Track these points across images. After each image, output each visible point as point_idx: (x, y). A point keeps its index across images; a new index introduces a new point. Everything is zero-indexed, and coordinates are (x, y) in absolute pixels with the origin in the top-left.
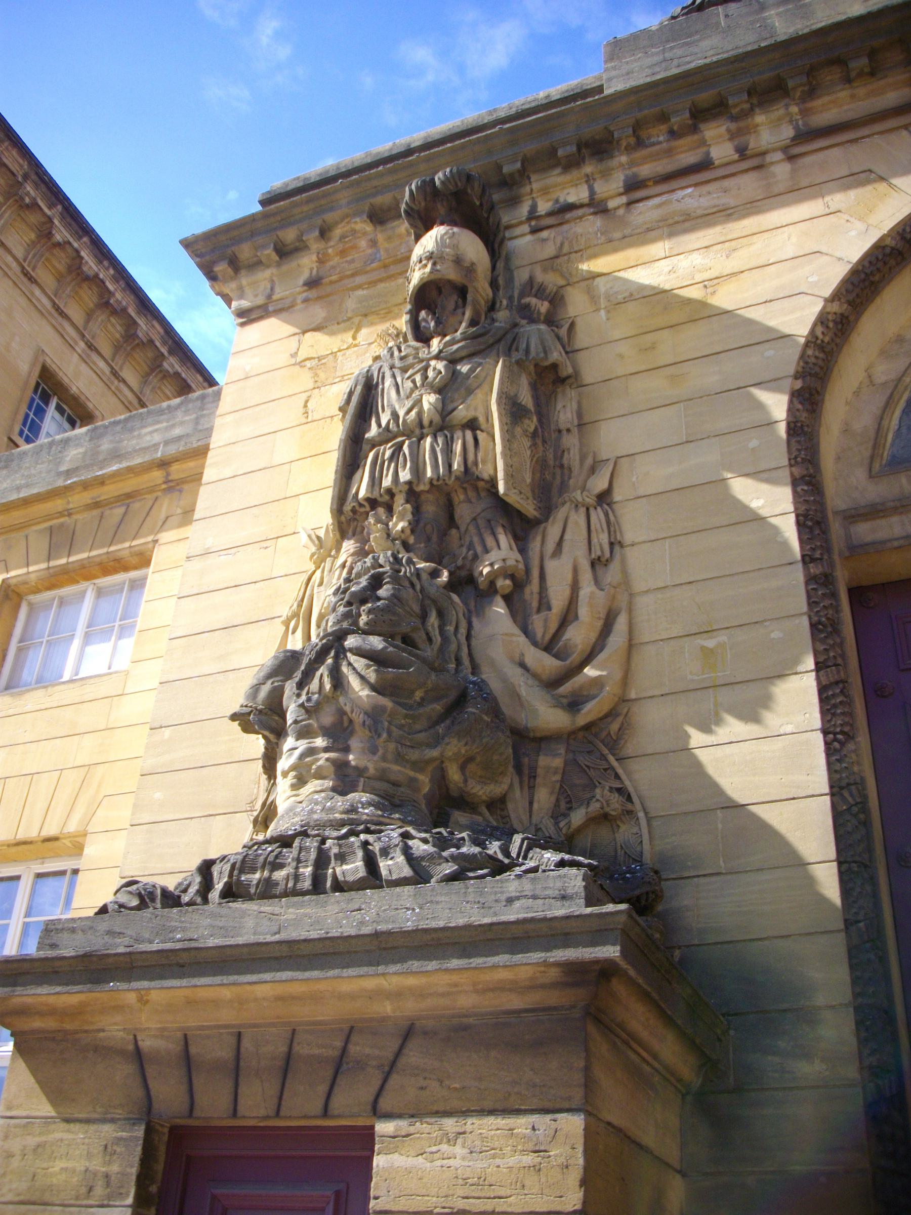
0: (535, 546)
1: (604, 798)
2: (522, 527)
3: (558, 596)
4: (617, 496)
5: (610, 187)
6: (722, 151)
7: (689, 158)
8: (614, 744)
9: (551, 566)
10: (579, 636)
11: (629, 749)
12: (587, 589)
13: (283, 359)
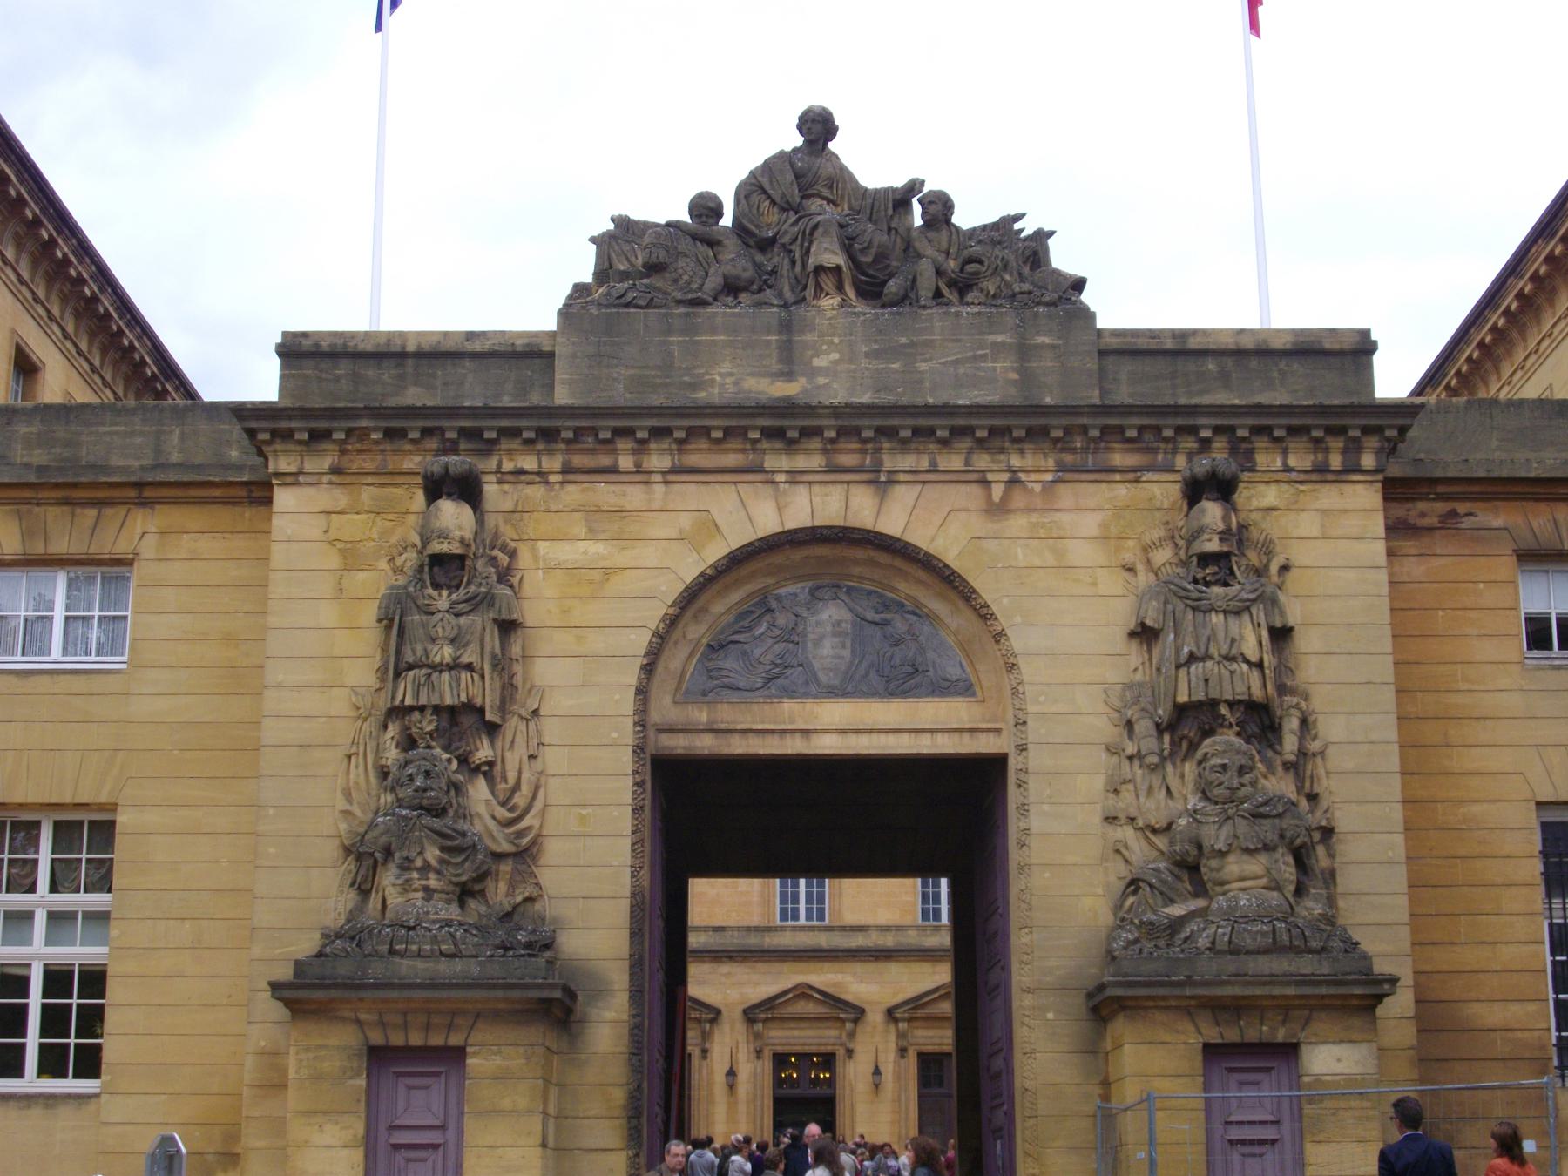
0: (499, 744)
1: (534, 891)
3: (512, 777)
5: (553, 463)
6: (626, 462)
7: (605, 460)
8: (535, 858)
9: (508, 754)
10: (520, 800)
11: (541, 862)
12: (526, 776)
13: (316, 533)
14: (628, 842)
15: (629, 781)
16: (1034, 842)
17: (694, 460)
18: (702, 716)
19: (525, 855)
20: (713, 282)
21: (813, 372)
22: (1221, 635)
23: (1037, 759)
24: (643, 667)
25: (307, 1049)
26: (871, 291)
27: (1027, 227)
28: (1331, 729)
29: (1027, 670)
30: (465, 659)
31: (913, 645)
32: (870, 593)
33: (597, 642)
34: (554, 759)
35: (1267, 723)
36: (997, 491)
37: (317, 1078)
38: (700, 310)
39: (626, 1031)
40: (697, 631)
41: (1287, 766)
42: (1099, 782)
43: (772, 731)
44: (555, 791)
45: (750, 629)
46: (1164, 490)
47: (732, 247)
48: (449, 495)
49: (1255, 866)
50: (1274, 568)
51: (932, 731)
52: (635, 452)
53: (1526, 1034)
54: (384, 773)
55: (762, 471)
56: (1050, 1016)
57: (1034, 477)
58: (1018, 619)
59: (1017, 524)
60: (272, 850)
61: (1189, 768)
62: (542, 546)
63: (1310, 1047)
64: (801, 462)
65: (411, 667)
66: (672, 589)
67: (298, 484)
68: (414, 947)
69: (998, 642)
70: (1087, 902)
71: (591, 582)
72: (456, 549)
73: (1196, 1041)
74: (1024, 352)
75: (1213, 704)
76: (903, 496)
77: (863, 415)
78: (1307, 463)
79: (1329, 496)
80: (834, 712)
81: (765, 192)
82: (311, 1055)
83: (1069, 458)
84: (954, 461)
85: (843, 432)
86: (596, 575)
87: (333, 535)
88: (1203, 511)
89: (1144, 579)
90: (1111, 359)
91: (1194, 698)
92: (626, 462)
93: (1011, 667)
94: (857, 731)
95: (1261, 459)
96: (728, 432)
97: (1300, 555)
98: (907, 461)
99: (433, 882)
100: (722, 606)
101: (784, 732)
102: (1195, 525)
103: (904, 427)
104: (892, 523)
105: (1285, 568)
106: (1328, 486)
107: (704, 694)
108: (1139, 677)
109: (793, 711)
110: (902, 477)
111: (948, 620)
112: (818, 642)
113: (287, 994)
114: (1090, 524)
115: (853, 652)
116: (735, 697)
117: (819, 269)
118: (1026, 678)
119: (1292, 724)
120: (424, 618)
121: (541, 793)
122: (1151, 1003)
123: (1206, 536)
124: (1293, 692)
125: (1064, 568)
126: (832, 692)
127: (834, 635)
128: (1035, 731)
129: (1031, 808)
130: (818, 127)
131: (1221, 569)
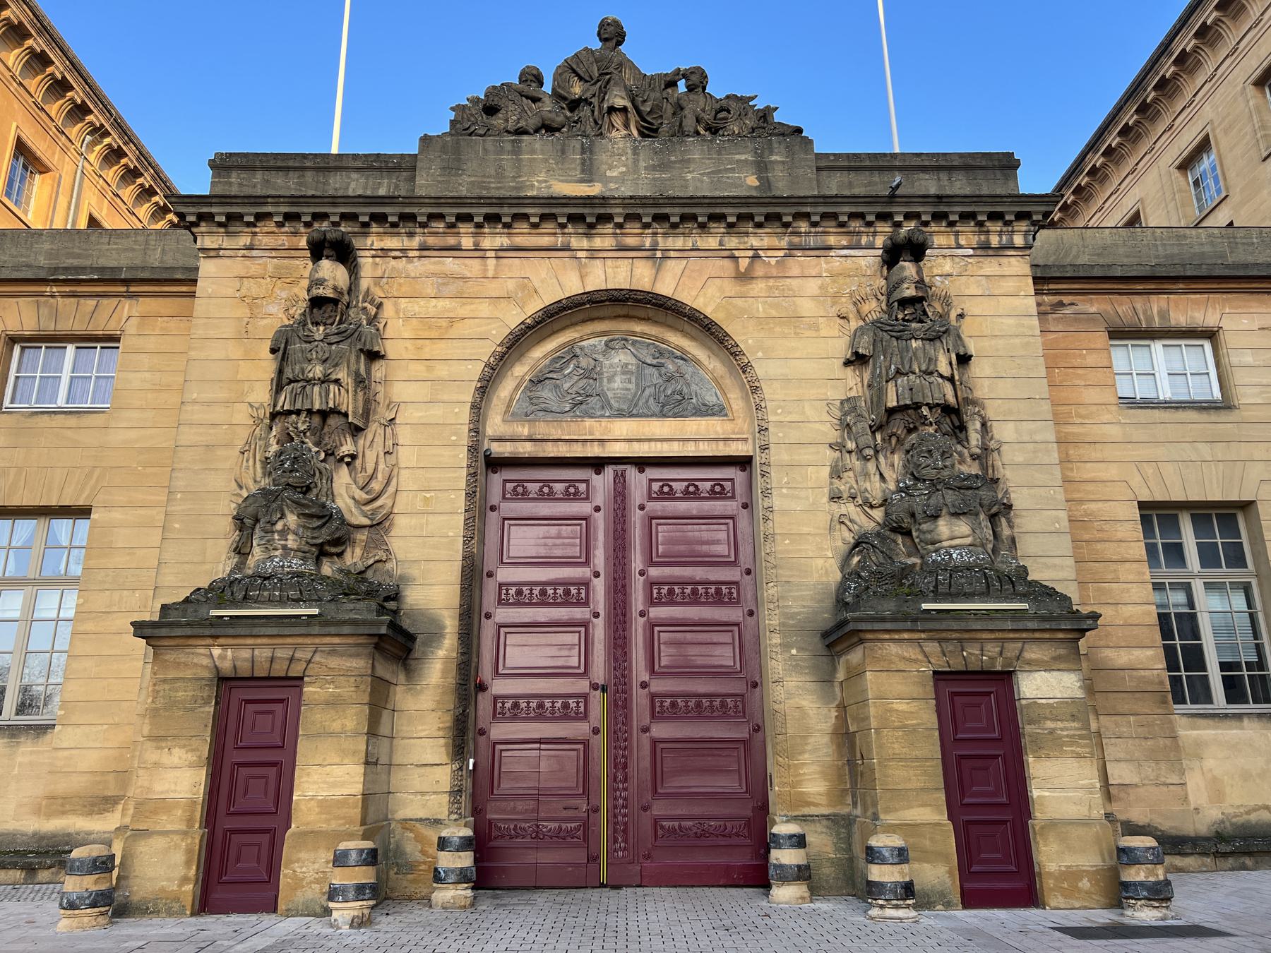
0: (361, 442)
1: (381, 555)
2: (356, 431)
3: (370, 467)
4: (397, 421)
6: (467, 242)
7: (451, 241)
8: (387, 531)
9: (368, 453)
10: (376, 486)
11: (392, 534)
12: (381, 466)
14: (461, 519)
15: (464, 472)
16: (777, 517)
17: (519, 241)
18: (525, 431)
19: (380, 525)
20: (532, 122)
21: (606, 180)
22: (920, 354)
23: (777, 455)
24: (477, 389)
25: (164, 681)
26: (649, 131)
27: (760, 104)
28: (1003, 432)
29: (767, 391)
30: (333, 377)
31: (681, 381)
32: (649, 345)
33: (442, 371)
34: (406, 456)
35: (957, 424)
36: (744, 263)
37: (171, 705)
38: (525, 137)
39: (454, 666)
40: (521, 370)
41: (974, 457)
42: (826, 471)
43: (577, 441)
44: (406, 479)
45: (561, 369)
46: (868, 260)
47: (547, 100)
48: (327, 257)
49: (963, 527)
50: (953, 315)
51: (695, 440)
52: (475, 235)
53: (1147, 673)
54: (266, 461)
55: (566, 248)
56: (794, 652)
57: (770, 253)
58: (760, 354)
59: (758, 287)
60: (177, 526)
61: (897, 459)
62: (403, 303)
63: (1025, 674)
64: (598, 243)
65: (291, 382)
66: (499, 333)
67: (218, 257)
68: (266, 593)
69: (744, 372)
70: (820, 562)
71: (440, 328)
72: (330, 294)
73: (927, 669)
74: (762, 167)
75: (917, 406)
76: (674, 268)
77: (644, 205)
78: (975, 240)
79: (990, 266)
80: (623, 427)
81: (574, 71)
82: (167, 687)
83: (796, 240)
84: (712, 242)
85: (629, 217)
86: (444, 323)
87: (243, 292)
88: (903, 268)
89: (855, 324)
90: (825, 173)
91: (901, 403)
92: (467, 242)
93: (755, 390)
94: (639, 441)
95: (938, 240)
96: (543, 217)
97: (971, 307)
98: (679, 242)
99: (291, 542)
100: (540, 353)
101: (585, 441)
102: (894, 278)
103: (673, 215)
104: (665, 288)
105: (961, 316)
106: (989, 259)
107: (527, 415)
108: (853, 394)
109: (593, 427)
110: (672, 254)
111: (706, 363)
112: (610, 380)
113: (148, 632)
114: (812, 286)
115: (637, 385)
116: (549, 417)
117: (612, 109)
118: (766, 396)
119: (974, 427)
120: (304, 345)
121: (394, 481)
122: (887, 636)
123: (905, 286)
124: (974, 403)
125: (794, 319)
126: (621, 414)
127: (624, 373)
128: (774, 435)
129: (774, 493)
130: (612, 34)
131: (911, 316)
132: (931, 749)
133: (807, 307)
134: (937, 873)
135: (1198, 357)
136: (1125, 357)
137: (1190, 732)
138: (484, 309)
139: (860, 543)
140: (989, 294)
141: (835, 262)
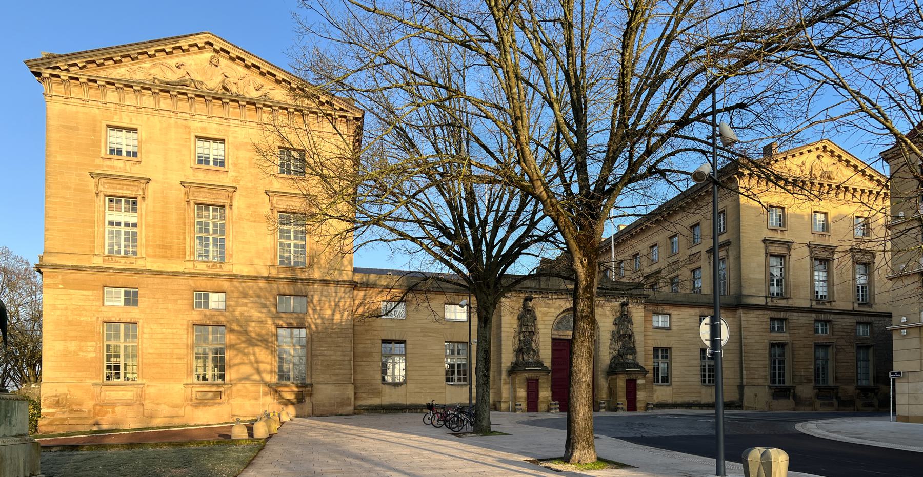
28: (637, 338)
34: (541, 339)
125: (605, 315)
132: (625, 390)
133: (608, 313)
134: (625, 407)
135: (667, 318)
136: (655, 318)
137: (655, 388)
138: (553, 310)
139: (614, 357)
140: (637, 312)
141: (613, 304)
